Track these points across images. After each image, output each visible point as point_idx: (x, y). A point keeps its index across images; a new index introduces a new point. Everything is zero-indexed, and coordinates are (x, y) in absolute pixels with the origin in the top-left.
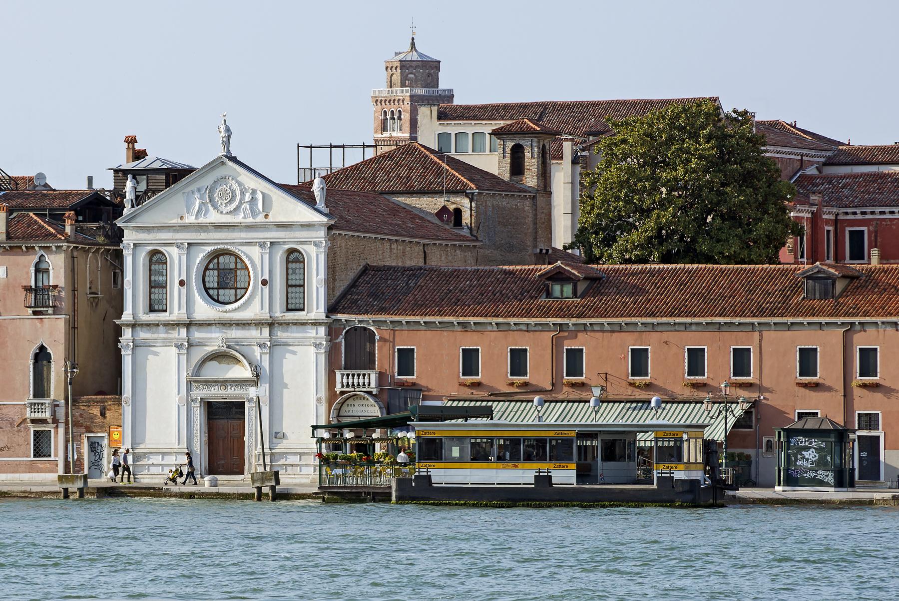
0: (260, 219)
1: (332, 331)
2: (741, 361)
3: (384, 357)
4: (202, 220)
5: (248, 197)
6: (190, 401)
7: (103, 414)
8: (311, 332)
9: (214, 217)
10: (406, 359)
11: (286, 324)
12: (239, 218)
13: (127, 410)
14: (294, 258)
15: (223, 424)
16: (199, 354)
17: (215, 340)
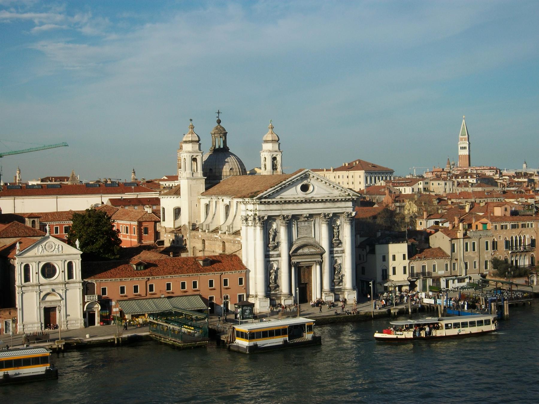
0: (61, 253)
1: (84, 284)
2: (195, 284)
3: (97, 291)
4: (42, 254)
5: (57, 247)
6: (40, 308)
7: (10, 314)
8: (78, 285)
9: (46, 253)
10: (104, 291)
11: (68, 283)
12: (54, 253)
13: (19, 313)
14: (70, 265)
15: (49, 314)
16: (42, 295)
17: (47, 289)
